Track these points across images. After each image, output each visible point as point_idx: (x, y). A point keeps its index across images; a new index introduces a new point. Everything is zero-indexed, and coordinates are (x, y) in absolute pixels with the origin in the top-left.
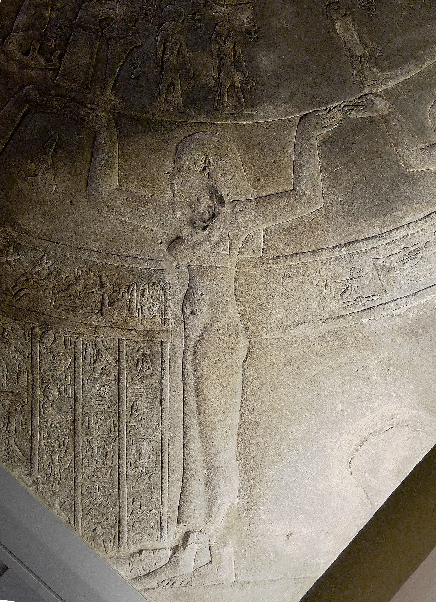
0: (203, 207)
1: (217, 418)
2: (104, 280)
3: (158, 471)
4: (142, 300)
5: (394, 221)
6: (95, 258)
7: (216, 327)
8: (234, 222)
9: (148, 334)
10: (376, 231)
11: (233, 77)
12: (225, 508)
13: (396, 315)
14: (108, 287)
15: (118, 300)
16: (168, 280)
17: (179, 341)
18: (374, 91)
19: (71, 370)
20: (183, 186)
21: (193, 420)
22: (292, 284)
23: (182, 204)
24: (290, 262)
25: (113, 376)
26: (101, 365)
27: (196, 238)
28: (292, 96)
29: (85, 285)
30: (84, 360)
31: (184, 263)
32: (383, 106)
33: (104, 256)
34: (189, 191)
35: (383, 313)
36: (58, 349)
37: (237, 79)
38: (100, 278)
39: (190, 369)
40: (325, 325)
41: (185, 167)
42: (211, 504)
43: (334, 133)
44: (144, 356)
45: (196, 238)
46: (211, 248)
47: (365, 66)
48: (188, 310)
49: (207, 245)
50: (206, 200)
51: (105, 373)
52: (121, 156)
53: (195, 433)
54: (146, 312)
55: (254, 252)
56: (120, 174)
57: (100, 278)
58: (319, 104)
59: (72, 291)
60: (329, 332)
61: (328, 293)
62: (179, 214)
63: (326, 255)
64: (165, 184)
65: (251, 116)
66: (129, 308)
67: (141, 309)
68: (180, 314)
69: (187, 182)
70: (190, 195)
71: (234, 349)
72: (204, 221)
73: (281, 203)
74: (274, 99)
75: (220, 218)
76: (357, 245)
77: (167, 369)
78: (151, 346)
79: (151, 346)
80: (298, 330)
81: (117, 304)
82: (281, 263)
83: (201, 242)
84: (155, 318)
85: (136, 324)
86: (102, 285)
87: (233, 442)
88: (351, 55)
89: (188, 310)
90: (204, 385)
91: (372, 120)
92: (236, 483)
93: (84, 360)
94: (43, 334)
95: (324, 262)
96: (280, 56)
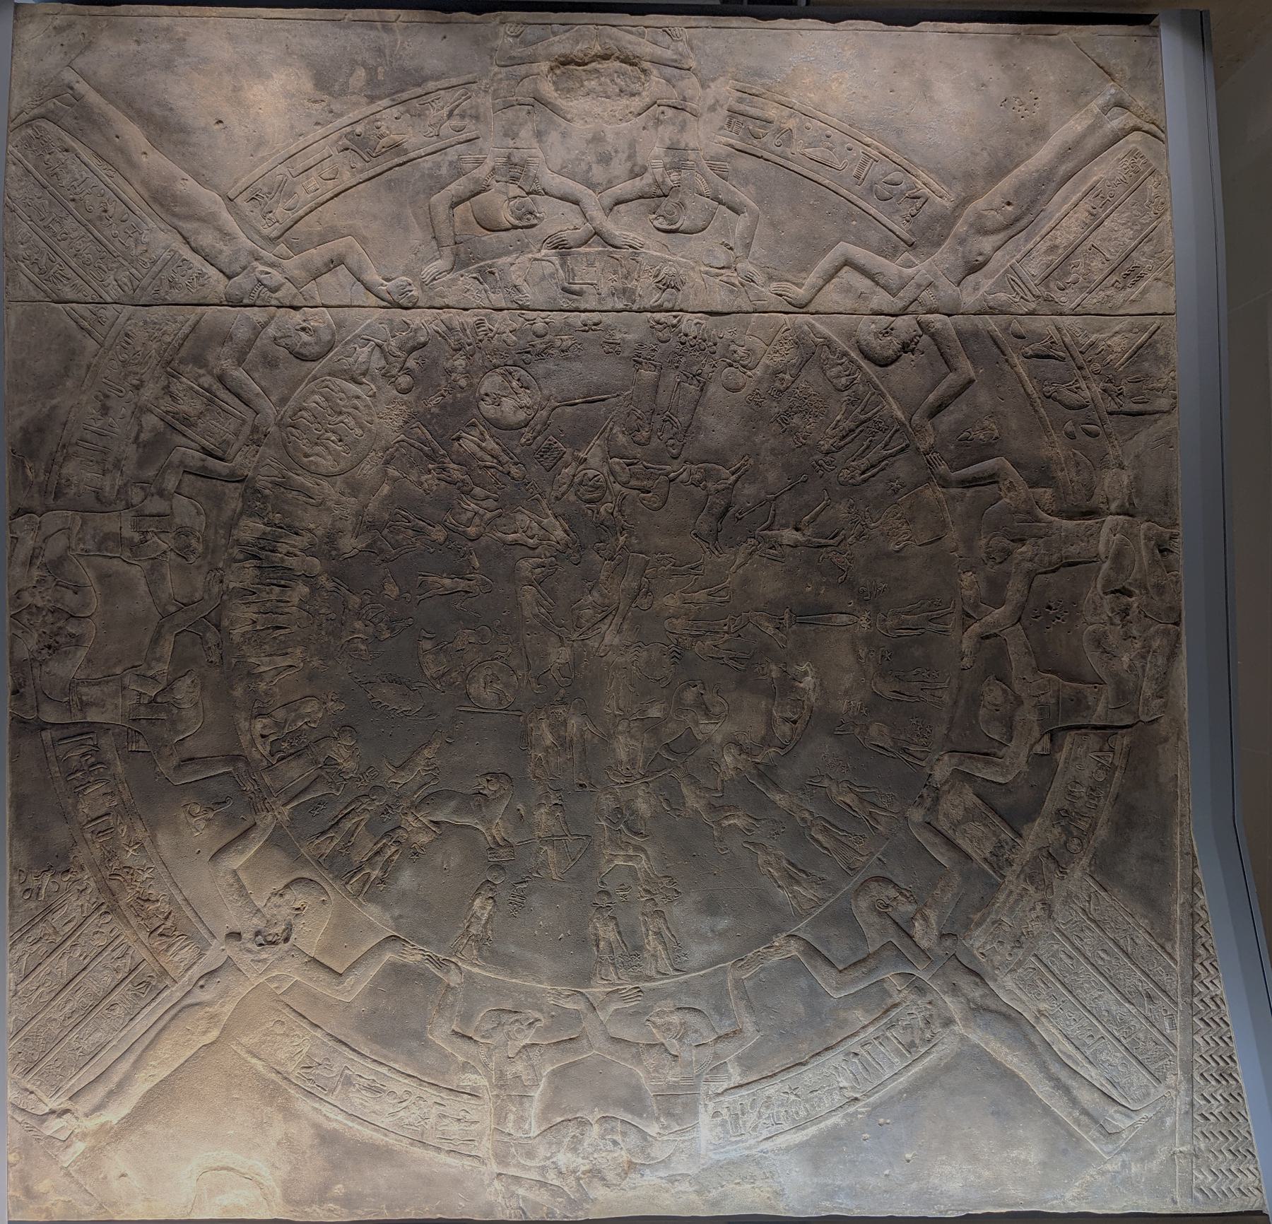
0: (275, 930)
1: (153, 1063)
2: (170, 917)
3: (88, 1058)
4: (181, 949)
5: (385, 1057)
6: (179, 899)
7: (208, 1009)
8: (282, 959)
9: (164, 973)
10: (365, 1051)
11: (374, 870)
12: (102, 1119)
13: (325, 1115)
14: (169, 923)
15: (168, 936)
16: (208, 953)
17: (179, 995)
18: (460, 964)
19: (100, 949)
20: (275, 906)
21: (138, 1049)
22: (279, 1030)
23: (264, 916)
24: (292, 1016)
25: (120, 976)
26: (119, 963)
27: (249, 945)
28: (401, 916)
29: (157, 909)
30: (113, 951)
31: (229, 953)
32: (454, 979)
33: (184, 903)
34: (275, 912)
35: (317, 1105)
36: (105, 930)
37: (376, 873)
38: (170, 913)
39: (167, 1017)
40: (274, 1074)
41: (287, 897)
42: (98, 1108)
43: (404, 965)
44: (149, 983)
45: (249, 945)
46: (252, 960)
47: (470, 943)
48: (201, 983)
49: (252, 957)
50: (279, 929)
51: (117, 971)
52: (257, 852)
53: (132, 1058)
54: (176, 959)
55: (276, 988)
56: (245, 862)
57: (170, 913)
58: (413, 938)
59: (147, 905)
60: (273, 1081)
61: (296, 1058)
62: (255, 921)
63: (319, 1034)
64: (267, 893)
65: (360, 905)
66: (169, 947)
67: (174, 954)
68: (195, 980)
69: (280, 906)
70: (274, 915)
71: (205, 1033)
72: (265, 941)
73: (323, 975)
74: (386, 907)
75: (276, 948)
76: (344, 1048)
77: (154, 1004)
78: (158, 981)
79: (158, 981)
80: (254, 1061)
81: (164, 938)
82: (286, 1011)
83: (249, 951)
84: (177, 967)
85: (163, 960)
86: (166, 918)
87: (147, 1086)
88: (468, 927)
89: (201, 983)
90: (165, 1035)
91: (439, 980)
92: (125, 1111)
93: (113, 951)
94: (106, 912)
95: (313, 1037)
96: (419, 885)
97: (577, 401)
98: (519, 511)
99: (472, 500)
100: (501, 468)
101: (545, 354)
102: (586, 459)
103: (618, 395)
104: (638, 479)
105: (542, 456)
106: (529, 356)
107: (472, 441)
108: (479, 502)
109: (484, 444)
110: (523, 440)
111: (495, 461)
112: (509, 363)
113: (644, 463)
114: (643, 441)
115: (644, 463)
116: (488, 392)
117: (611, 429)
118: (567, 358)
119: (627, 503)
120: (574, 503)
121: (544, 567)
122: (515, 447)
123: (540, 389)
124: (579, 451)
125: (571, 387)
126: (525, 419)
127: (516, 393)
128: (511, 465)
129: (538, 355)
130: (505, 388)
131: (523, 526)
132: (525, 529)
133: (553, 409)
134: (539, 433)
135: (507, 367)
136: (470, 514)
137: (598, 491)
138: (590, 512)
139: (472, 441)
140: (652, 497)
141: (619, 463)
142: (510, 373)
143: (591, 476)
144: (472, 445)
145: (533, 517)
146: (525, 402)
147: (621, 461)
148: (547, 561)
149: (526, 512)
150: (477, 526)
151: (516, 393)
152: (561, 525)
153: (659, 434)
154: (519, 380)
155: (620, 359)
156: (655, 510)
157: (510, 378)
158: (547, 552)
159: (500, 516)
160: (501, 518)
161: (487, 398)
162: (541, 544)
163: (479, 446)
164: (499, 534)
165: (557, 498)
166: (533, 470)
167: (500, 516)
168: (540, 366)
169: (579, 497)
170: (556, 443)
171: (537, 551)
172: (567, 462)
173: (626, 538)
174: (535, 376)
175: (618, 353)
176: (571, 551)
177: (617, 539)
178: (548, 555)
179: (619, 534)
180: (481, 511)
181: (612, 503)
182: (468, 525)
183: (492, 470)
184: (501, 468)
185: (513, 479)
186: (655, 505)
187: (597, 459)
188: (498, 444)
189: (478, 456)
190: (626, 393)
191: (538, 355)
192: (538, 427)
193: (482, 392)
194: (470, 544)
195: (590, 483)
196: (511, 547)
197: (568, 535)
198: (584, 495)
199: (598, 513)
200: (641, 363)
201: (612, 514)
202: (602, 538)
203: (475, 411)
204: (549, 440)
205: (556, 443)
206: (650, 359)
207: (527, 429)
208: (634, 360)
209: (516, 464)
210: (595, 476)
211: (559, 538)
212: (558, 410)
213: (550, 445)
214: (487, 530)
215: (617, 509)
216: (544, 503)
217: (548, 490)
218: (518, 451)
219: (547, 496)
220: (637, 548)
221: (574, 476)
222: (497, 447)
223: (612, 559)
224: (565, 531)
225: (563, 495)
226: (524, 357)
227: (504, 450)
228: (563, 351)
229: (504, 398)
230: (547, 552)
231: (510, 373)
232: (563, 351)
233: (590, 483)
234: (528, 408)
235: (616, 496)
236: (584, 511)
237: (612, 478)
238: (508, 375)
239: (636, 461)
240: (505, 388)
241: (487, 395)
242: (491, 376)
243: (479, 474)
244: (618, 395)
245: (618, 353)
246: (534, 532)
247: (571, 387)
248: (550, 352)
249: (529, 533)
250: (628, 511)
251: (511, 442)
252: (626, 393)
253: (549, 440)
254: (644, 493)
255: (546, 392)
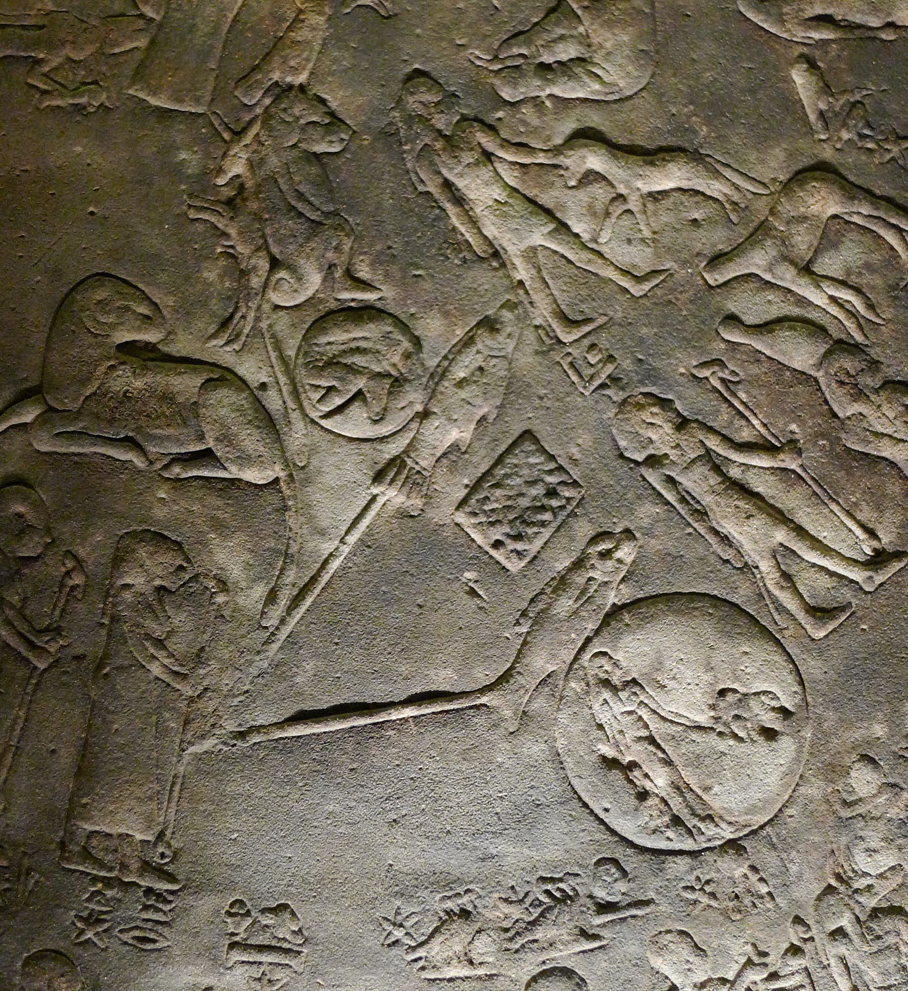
97: (409, 712)
98: (639, 279)
99: (825, 321)
100: (713, 443)
101: (537, 903)
102: (378, 477)
103: (242, 735)
104: (167, 398)
105: (552, 493)
106: (601, 894)
107: (827, 551)
108: (796, 311)
109: (781, 535)
110: (626, 553)
111: (734, 472)
112: (683, 863)
113: (139, 462)
114: (142, 552)
115: (139, 462)
116: (762, 745)
117: (272, 597)
118: (448, 885)
119: (215, 305)
120: (428, 306)
121: (544, 68)
122: (660, 529)
123: (557, 759)
124: (404, 515)
125: (432, 767)
126: (616, 638)
127: (651, 740)
128: (673, 454)
129: (566, 899)
130: (696, 761)
131: (626, 221)
132: (618, 209)
133: (505, 678)
134: (562, 583)
135: (688, 845)
136: (829, 264)
137: (335, 349)
138: (364, 272)
139: (827, 551)
140: (113, 326)
141: (245, 460)
142: (676, 821)
143: (356, 410)
144: (825, 535)
145: (586, 255)
146: (618, 708)
147: (234, 472)
148: (533, 87)
149: (610, 273)
150: (804, 218)
151: (651, 740)
152: (474, 222)
153: (77, 580)
154: (643, 795)
155: (232, 886)
156: (104, 276)
157: (676, 804)
158: (535, 121)
159: (717, 260)
160: (709, 252)
161: (770, 720)
162: (557, 151)
163: (800, 531)
164: (716, 188)
165: (490, 325)
166: (585, 439)
167: (717, 260)
168: (554, 854)
169: (404, 327)
170: (497, 544)
171: (569, 126)
172: (453, 469)
173: (220, 171)
174: (579, 811)
175: (238, 909)
176: (440, 122)
177: (251, 164)
178: (527, 111)
179: (249, 184)
180: (787, 277)
181: (277, 307)
182: (835, 226)
183: (746, 435)
184: (713, 443)
185: (665, 404)
186: (101, 294)
187: (330, 478)
188: (725, 540)
189: (800, 489)
190: (208, 744)
191: (566, 899)
192: (565, 604)
193: (786, 745)
194: (828, 154)
195: (361, 383)
196: (671, 141)
197: (447, 185)
198: (386, 336)
199: (331, 266)
200: (147, 867)
201: (275, 264)
202: (314, 170)
203: (812, 667)
204: (519, 554)
205: (497, 544)
206: (108, 883)
207: (612, 598)
208: (171, 878)
209: (653, 461)
210: (340, 410)
211: (485, 173)
212: (484, 675)
213: (518, 537)
214: (761, 207)
215: (256, 282)
216: (542, 313)
217: (526, 360)
218: (648, 511)
219: (530, 336)
220: (179, 133)
221: (425, 415)
222: (729, 527)
223: (282, 91)
224: (459, 200)
225: (468, 341)
226: (622, 886)
227: (702, 514)
228: (465, 914)
229: (703, 719)
230: (535, 121)
231: (676, 821)
232: (465, 914)
233: (361, 383)
234: (606, 683)
235: (256, 332)
236: (387, 275)
237: (273, 401)
238: (684, 815)
239: (176, 470)
240: (696, 761)
241: (770, 734)
242: (752, 810)
243: (799, 420)
244: (242, 735)
245: (238, 909)
246: (583, 196)
247: (432, 767)
248: (516, 912)
249: (600, 192)
250: (211, 274)
251: (670, 546)
252: (208, 744)
253: (519, 554)
254: (150, 347)
255: (535, 749)
